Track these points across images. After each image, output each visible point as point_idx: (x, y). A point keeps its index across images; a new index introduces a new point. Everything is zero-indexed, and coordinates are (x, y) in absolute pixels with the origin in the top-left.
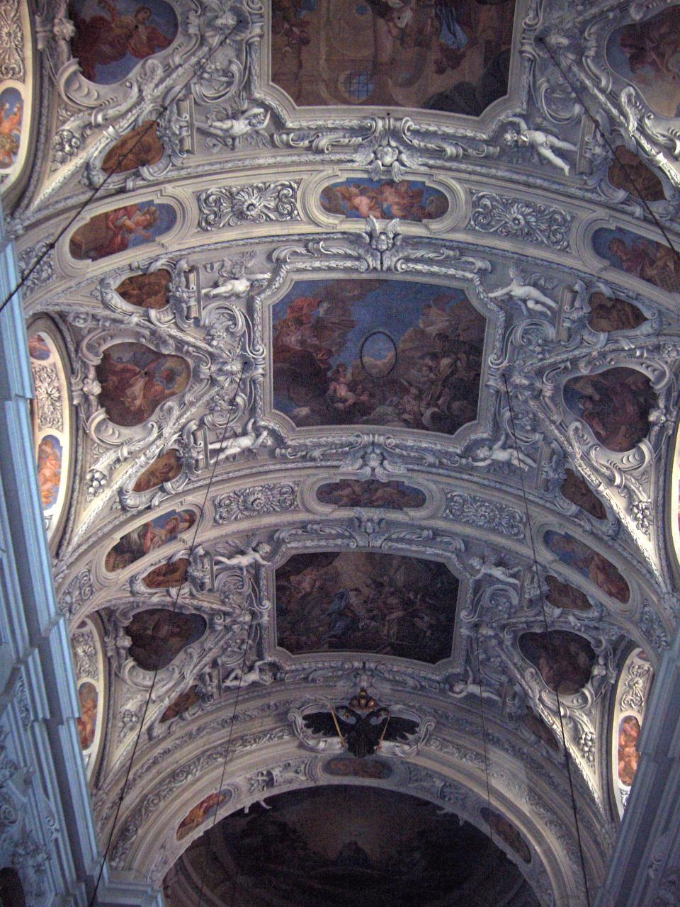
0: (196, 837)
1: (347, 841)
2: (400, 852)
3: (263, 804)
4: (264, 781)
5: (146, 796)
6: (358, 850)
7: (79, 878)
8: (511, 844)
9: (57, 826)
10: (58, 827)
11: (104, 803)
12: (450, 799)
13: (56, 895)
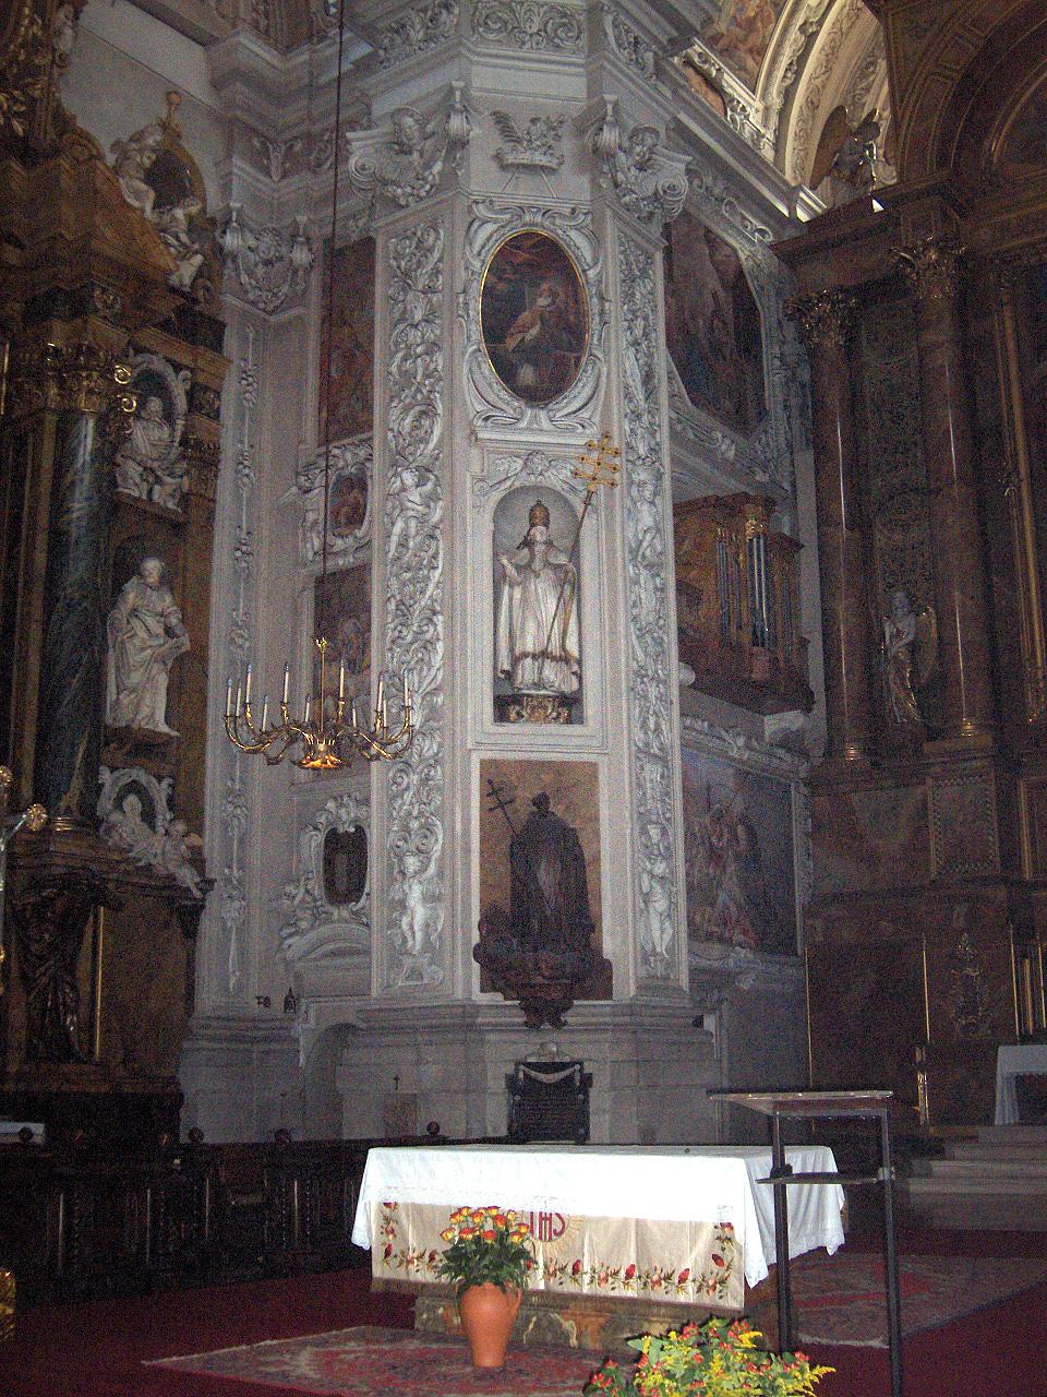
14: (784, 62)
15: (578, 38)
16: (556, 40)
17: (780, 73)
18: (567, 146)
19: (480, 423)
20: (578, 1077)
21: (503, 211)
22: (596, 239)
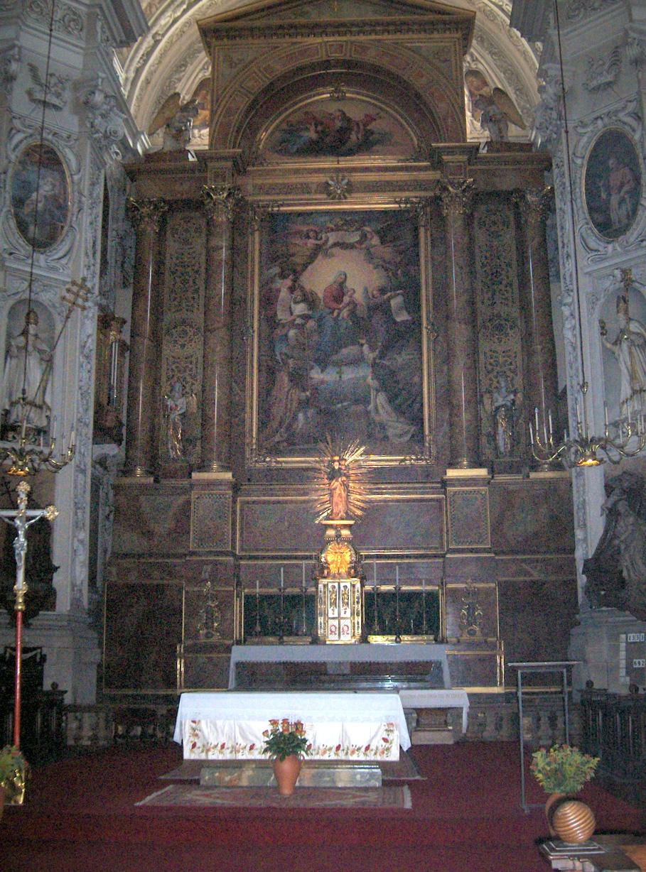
14: (141, 52)
15: (81, 30)
16: (70, 29)
17: (137, 59)
18: (68, 95)
19: (6, 256)
20: (39, 656)
21: (30, 127)
22: (80, 159)
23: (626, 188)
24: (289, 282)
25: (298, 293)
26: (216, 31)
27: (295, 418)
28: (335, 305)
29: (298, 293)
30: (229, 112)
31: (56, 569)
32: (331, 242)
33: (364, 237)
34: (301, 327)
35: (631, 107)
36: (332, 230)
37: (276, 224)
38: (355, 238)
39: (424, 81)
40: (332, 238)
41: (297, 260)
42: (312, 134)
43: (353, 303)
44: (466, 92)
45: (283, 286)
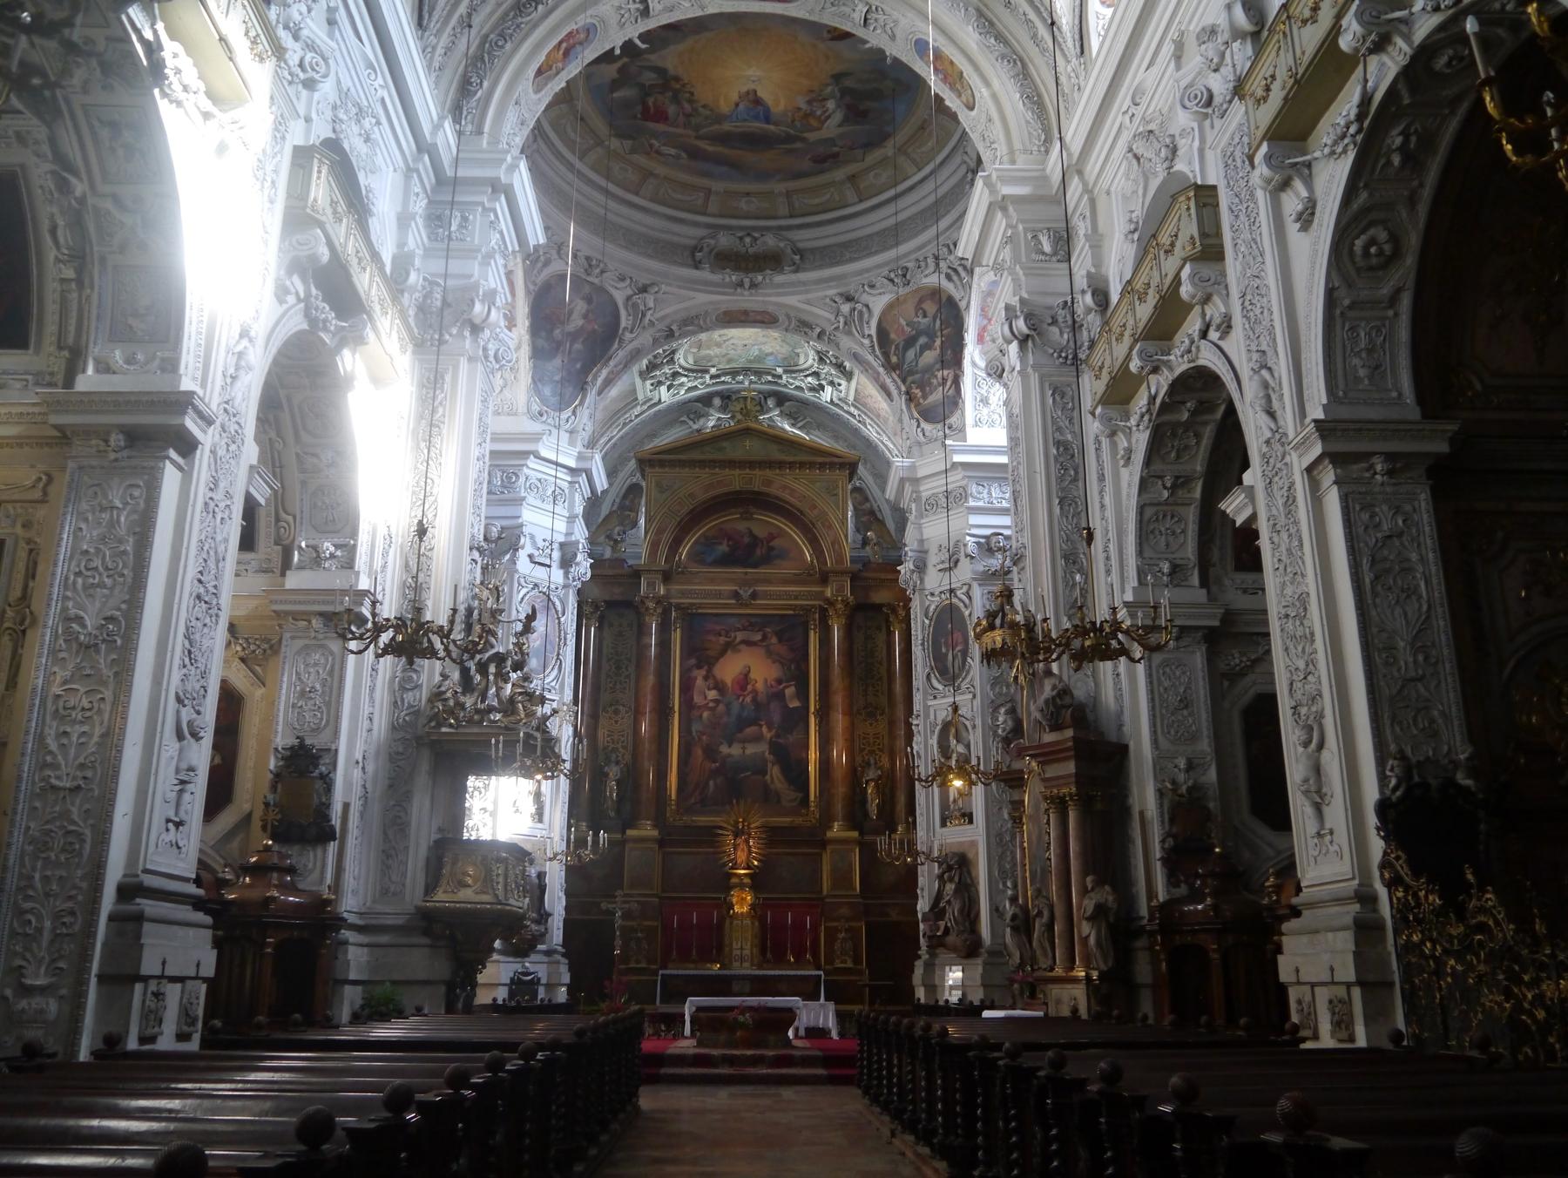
0: (557, 89)
1: (744, 89)
2: (809, 102)
3: (638, 42)
4: (638, 10)
5: (486, 36)
6: (758, 101)
7: (420, 149)
8: (952, 87)
9: (380, 81)
10: (382, 83)
11: (434, 48)
12: (875, 29)
13: (395, 170)
18: (556, 555)
23: (959, 648)
24: (703, 672)
25: (711, 681)
26: (650, 461)
27: (707, 784)
28: (739, 692)
29: (711, 681)
30: (660, 532)
31: (549, 915)
32: (738, 640)
33: (765, 638)
34: (712, 709)
35: (965, 589)
36: (739, 630)
37: (693, 620)
38: (758, 637)
39: (816, 512)
40: (740, 636)
41: (710, 653)
42: (723, 548)
43: (755, 691)
44: (850, 507)
45: (699, 675)
